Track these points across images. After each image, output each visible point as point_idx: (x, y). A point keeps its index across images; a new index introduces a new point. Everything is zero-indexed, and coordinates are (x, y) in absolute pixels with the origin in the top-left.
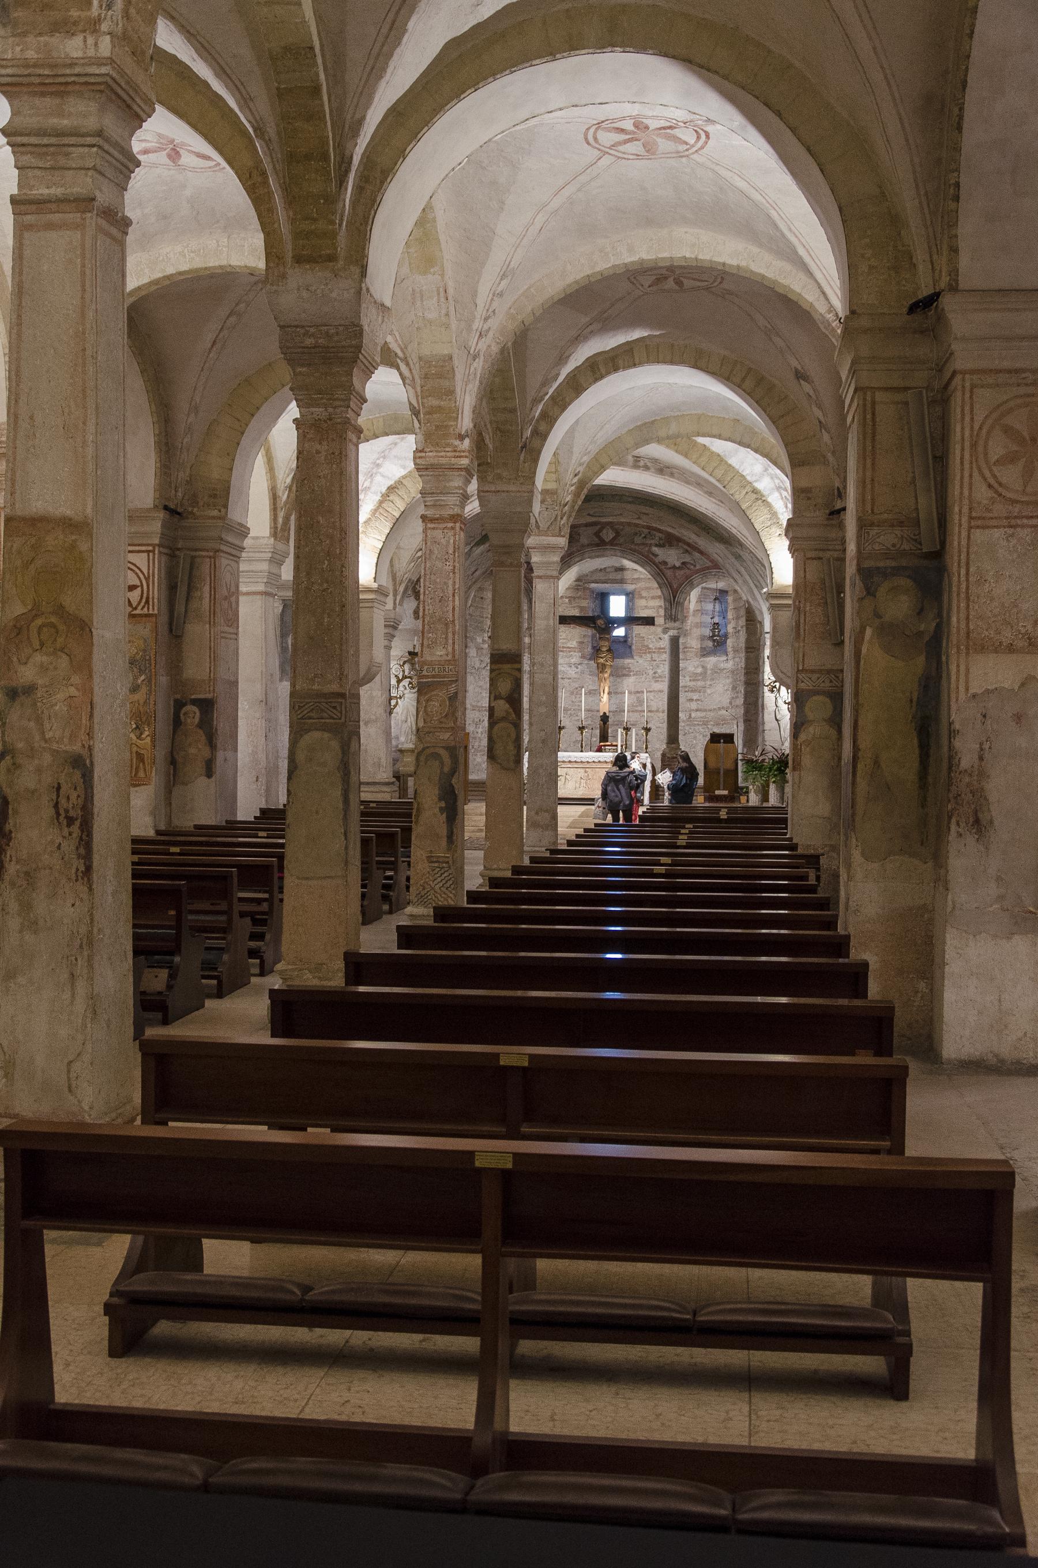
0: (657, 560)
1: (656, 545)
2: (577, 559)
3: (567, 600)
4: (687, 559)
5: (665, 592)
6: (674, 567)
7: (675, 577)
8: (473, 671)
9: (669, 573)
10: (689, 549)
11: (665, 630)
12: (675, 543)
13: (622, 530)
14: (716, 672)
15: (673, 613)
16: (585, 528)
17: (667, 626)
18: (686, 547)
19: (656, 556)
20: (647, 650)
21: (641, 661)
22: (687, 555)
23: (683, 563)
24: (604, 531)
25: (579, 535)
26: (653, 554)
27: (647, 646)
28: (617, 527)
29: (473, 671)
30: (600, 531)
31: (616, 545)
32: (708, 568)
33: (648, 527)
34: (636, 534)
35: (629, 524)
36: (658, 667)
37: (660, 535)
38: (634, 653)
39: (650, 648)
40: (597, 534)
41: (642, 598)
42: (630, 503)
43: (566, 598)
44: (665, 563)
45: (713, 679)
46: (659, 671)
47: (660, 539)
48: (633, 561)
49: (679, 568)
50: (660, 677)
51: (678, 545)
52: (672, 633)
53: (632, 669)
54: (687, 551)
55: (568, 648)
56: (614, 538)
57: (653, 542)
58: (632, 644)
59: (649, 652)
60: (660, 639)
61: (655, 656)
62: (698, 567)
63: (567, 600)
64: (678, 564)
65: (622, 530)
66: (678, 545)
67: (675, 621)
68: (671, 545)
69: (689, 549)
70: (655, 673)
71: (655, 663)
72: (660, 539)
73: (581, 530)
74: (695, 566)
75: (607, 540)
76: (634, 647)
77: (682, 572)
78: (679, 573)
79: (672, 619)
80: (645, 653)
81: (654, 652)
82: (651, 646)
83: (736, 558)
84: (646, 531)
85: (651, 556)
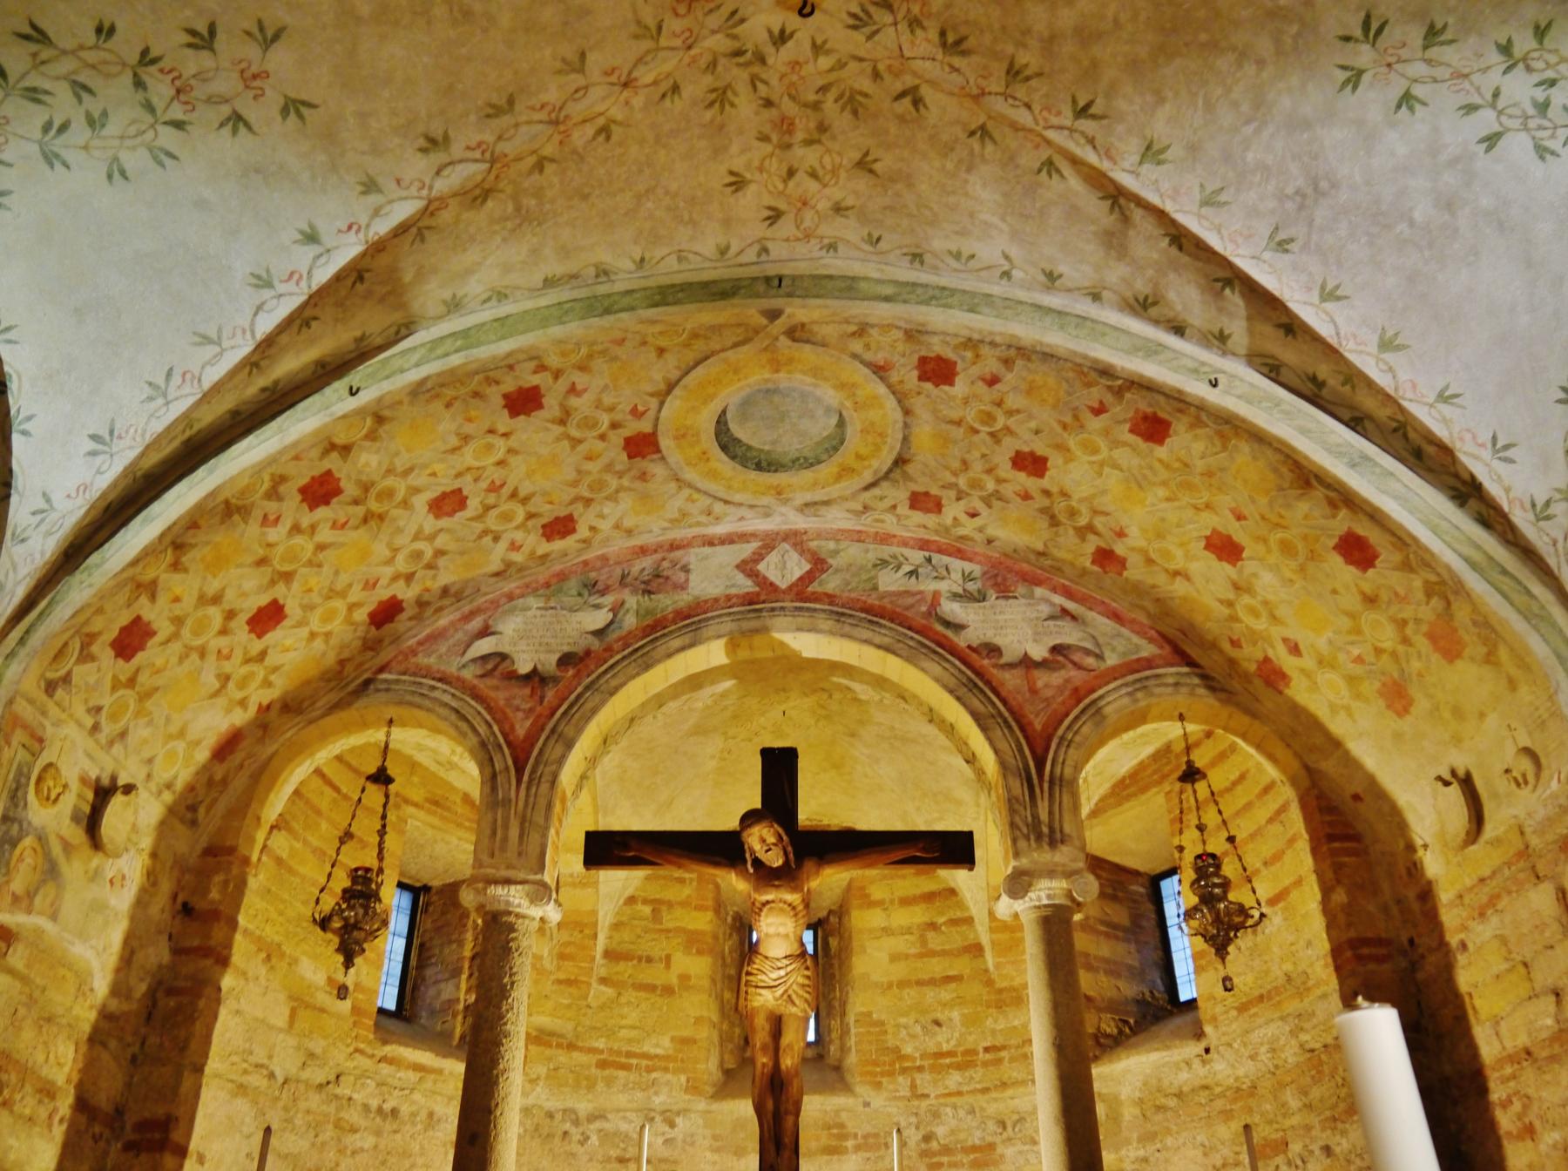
0: (961, 640)
1: (955, 596)
2: (676, 643)
3: (647, 910)
4: (1069, 635)
5: (1003, 745)
6: (1026, 663)
7: (1034, 691)
8: (256, 1080)
9: (1011, 681)
10: (1071, 606)
11: (1018, 883)
12: (1021, 589)
13: (836, 552)
14: (1160, 1108)
15: (1044, 816)
16: (707, 550)
17: (1024, 862)
18: (1059, 600)
19: (959, 627)
20: (894, 1063)
21: (878, 1101)
22: (1066, 624)
23: (1056, 649)
24: (773, 558)
25: (686, 569)
26: (947, 624)
27: (897, 1050)
28: (813, 545)
29: (256, 1080)
30: (758, 557)
31: (816, 598)
32: (1148, 663)
33: (924, 545)
34: (883, 563)
35: (859, 537)
36: (936, 1115)
37: (968, 567)
38: (855, 1079)
39: (902, 1058)
40: (748, 567)
41: (871, 904)
42: (887, 299)
43: (645, 902)
44: (993, 650)
45: (1147, 1138)
46: (941, 1131)
47: (967, 577)
48: (879, 647)
49: (1043, 664)
50: (946, 1150)
51: (1031, 596)
52: (1046, 892)
53: (851, 1127)
54: (1065, 612)
55: (645, 1056)
56: (808, 578)
57: (943, 586)
58: (844, 1049)
59: (904, 1071)
60: (937, 1023)
61: (924, 1081)
62: (1112, 660)
63: (647, 910)
64: (1038, 652)
65: (836, 552)
66: (1031, 596)
67: (1053, 844)
68: (1005, 593)
69: (1071, 606)
70: (927, 1138)
71: (924, 1104)
72: (967, 577)
73: (693, 556)
74: (1100, 657)
75: (783, 585)
76: (852, 1059)
77: (1056, 678)
78: (1043, 679)
79: (1039, 837)
80: (891, 1074)
81: (920, 1069)
82: (908, 1049)
83: (1353, 465)
84: (917, 556)
85: (939, 628)
